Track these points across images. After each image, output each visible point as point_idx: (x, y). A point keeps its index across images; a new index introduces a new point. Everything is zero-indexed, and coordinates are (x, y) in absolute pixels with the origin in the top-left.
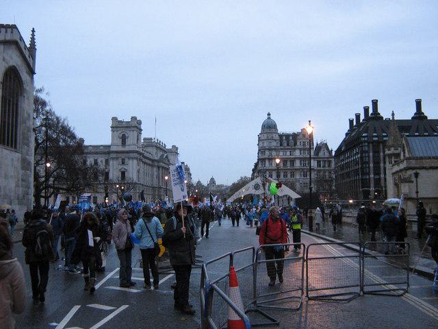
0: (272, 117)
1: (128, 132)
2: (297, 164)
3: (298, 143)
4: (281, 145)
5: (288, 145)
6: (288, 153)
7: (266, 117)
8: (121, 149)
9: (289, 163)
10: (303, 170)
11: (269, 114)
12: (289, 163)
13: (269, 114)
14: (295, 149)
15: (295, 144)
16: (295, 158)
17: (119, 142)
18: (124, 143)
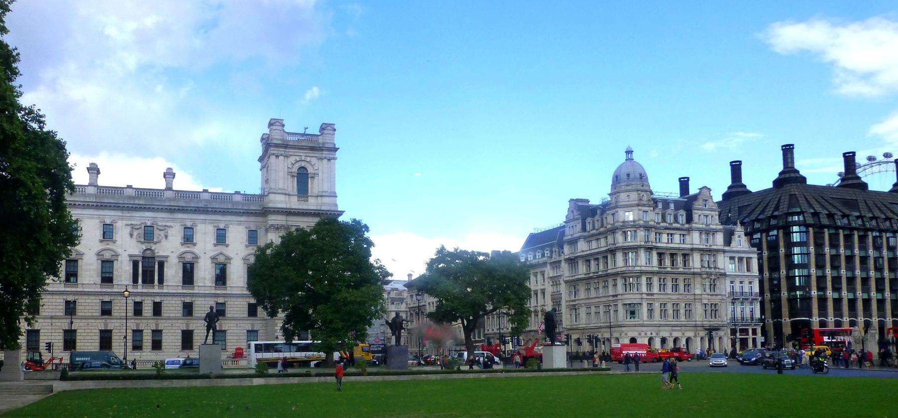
0: (636, 157)
1: (314, 161)
2: (696, 262)
3: (696, 217)
4: (664, 220)
5: (676, 221)
6: (677, 238)
7: (623, 158)
8: (294, 203)
9: (680, 259)
10: (709, 274)
11: (629, 152)
12: (680, 259)
13: (629, 152)
14: (689, 230)
15: (689, 219)
16: (692, 250)
17: (292, 185)
18: (303, 191)
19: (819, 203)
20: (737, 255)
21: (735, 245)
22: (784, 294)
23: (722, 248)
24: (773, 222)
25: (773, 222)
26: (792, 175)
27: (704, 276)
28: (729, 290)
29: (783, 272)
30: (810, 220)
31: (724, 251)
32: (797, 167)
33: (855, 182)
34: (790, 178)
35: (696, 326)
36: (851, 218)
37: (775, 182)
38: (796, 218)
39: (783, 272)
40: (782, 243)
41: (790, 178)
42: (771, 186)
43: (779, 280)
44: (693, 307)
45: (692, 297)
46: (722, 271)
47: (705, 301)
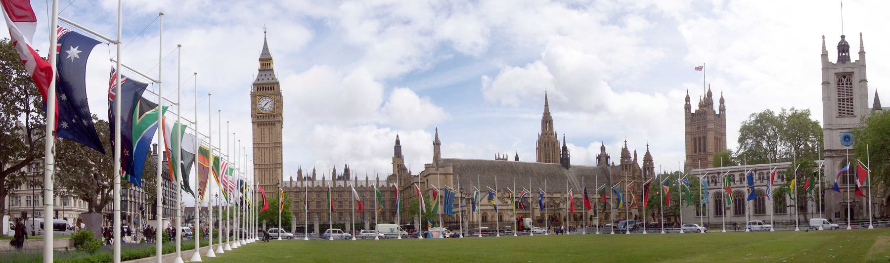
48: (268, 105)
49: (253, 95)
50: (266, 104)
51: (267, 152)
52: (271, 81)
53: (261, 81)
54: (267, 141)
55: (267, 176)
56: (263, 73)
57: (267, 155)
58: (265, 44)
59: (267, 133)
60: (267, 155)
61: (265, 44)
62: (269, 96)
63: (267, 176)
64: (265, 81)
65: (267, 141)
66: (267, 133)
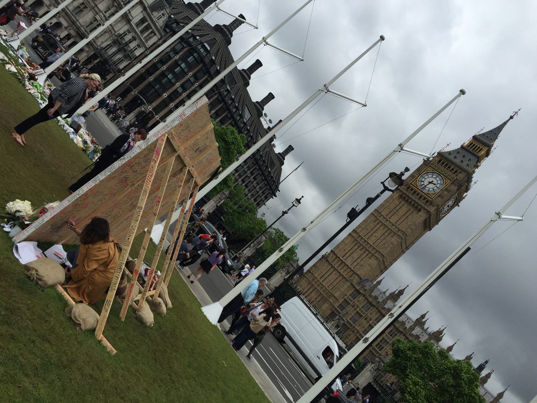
19: (221, 61)
20: (149, 22)
21: (156, 15)
22: (151, 78)
23: (147, 5)
24: (191, 40)
25: (191, 40)
26: (228, 33)
27: (116, 4)
28: (121, 32)
29: (164, 68)
30: (207, 60)
31: (145, 9)
32: (234, 33)
33: (246, 77)
34: (225, 33)
35: (74, 23)
36: (224, 86)
37: (217, 26)
38: (202, 50)
39: (164, 68)
40: (181, 54)
41: (225, 33)
42: (213, 26)
43: (158, 69)
44: (86, 11)
45: (93, 5)
46: (131, 18)
47: (98, 17)
48: (431, 186)
49: (427, 163)
50: (432, 183)
51: (381, 231)
52: (464, 165)
53: (451, 157)
54: (393, 220)
55: (356, 255)
56: (463, 152)
57: (378, 234)
58: (500, 128)
59: (401, 212)
60: (378, 234)
61: (500, 128)
62: (444, 177)
63: (356, 255)
64: (457, 161)
65: (393, 220)
66: (401, 212)
